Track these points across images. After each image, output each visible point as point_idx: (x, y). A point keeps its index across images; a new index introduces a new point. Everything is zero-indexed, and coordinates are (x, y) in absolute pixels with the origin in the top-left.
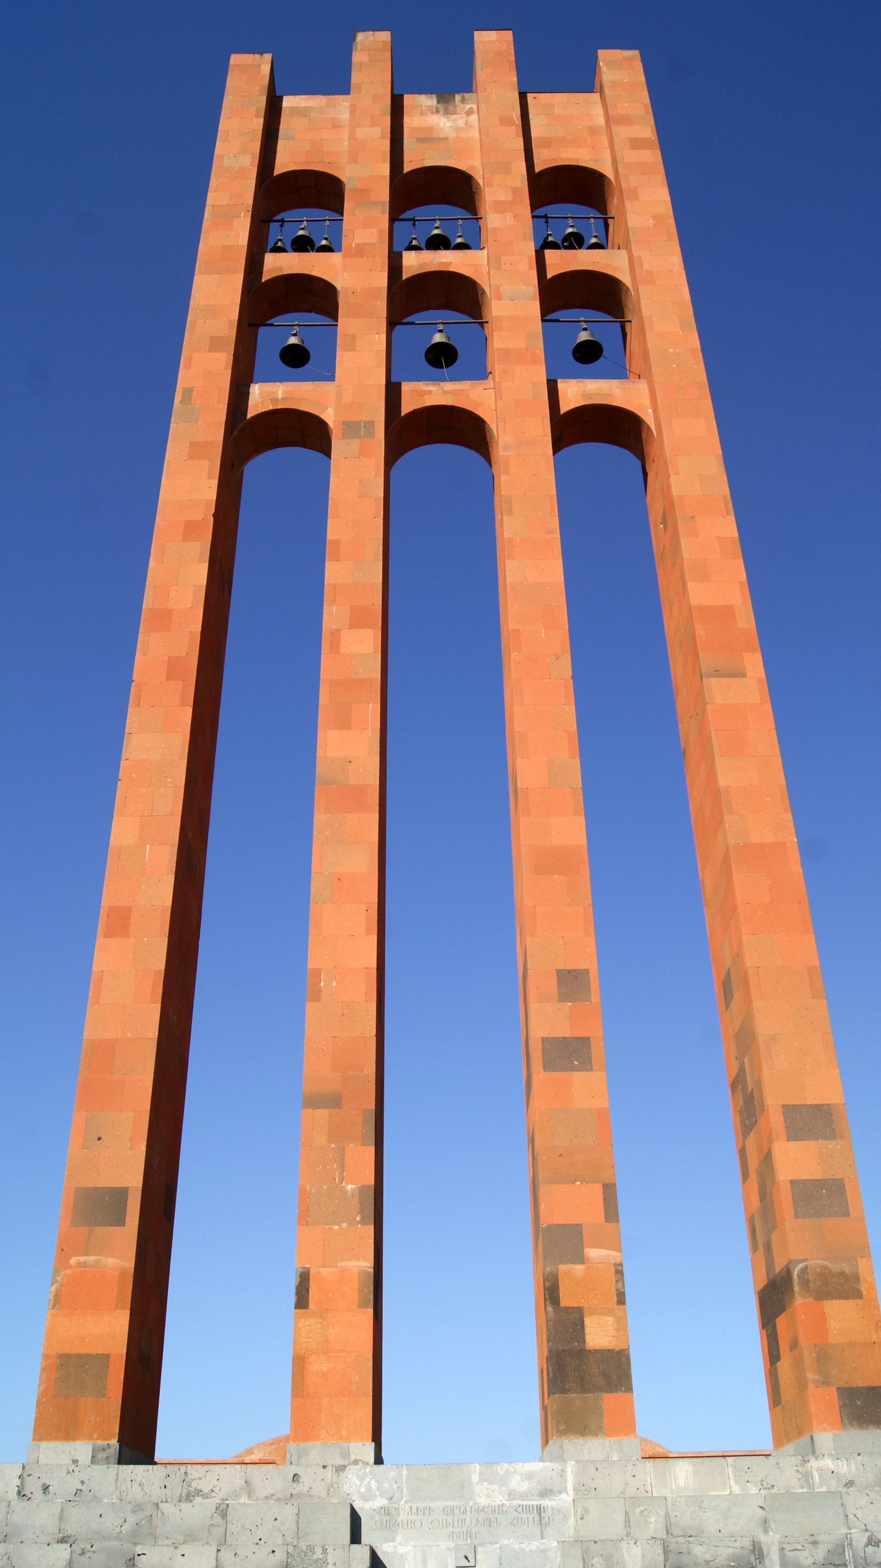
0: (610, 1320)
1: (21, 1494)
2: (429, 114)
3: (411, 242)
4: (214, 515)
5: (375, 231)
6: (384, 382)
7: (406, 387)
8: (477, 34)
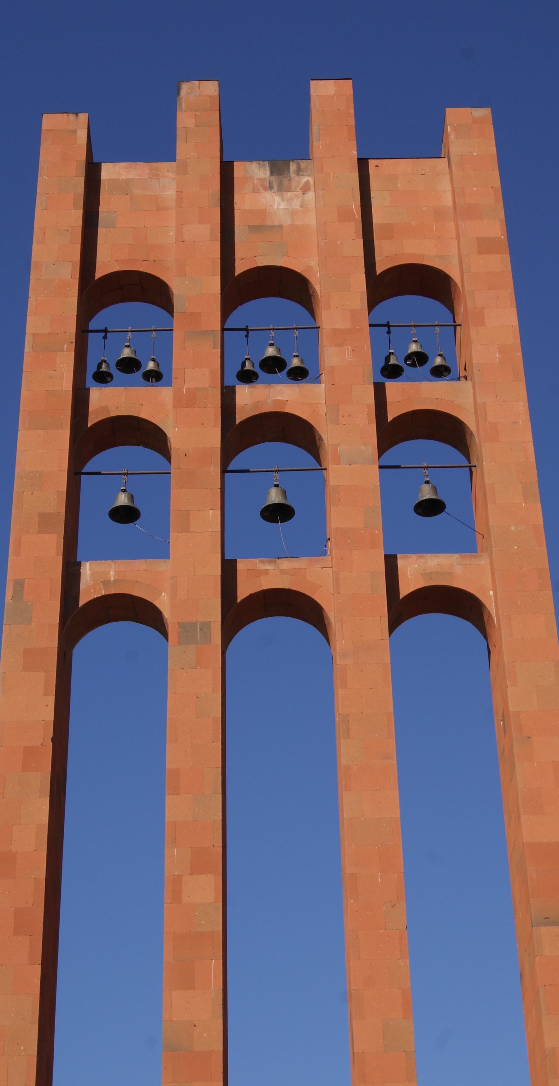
2: (262, 191)
3: (244, 364)
4: (53, 740)
7: (242, 566)
8: (314, 85)
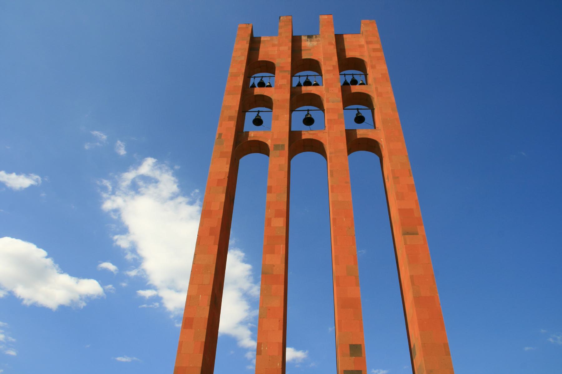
5: (286, 80)
6: (288, 131)
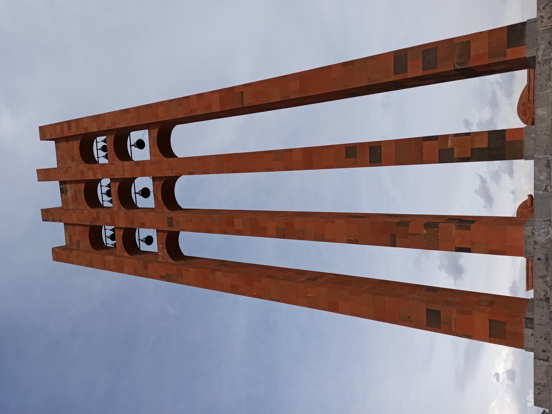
0: (476, 138)
1: (546, 360)
